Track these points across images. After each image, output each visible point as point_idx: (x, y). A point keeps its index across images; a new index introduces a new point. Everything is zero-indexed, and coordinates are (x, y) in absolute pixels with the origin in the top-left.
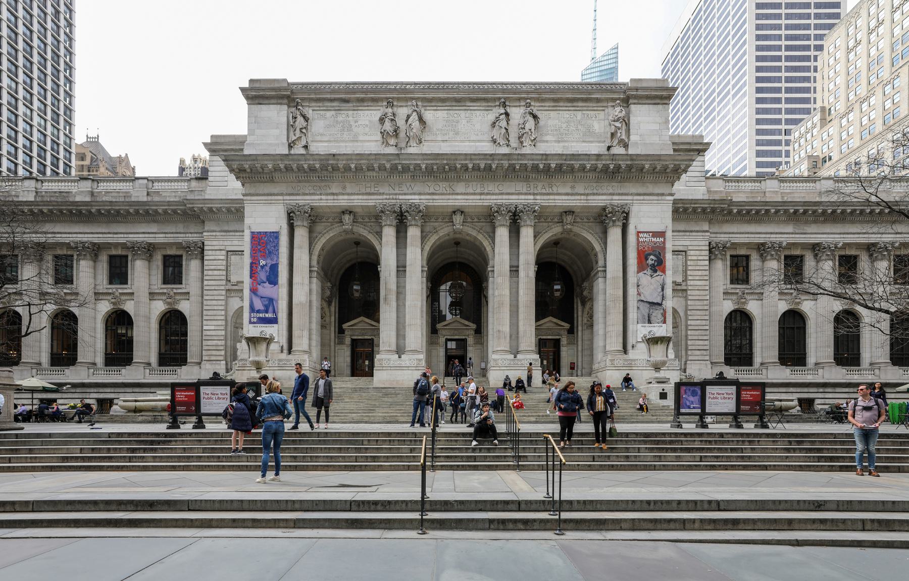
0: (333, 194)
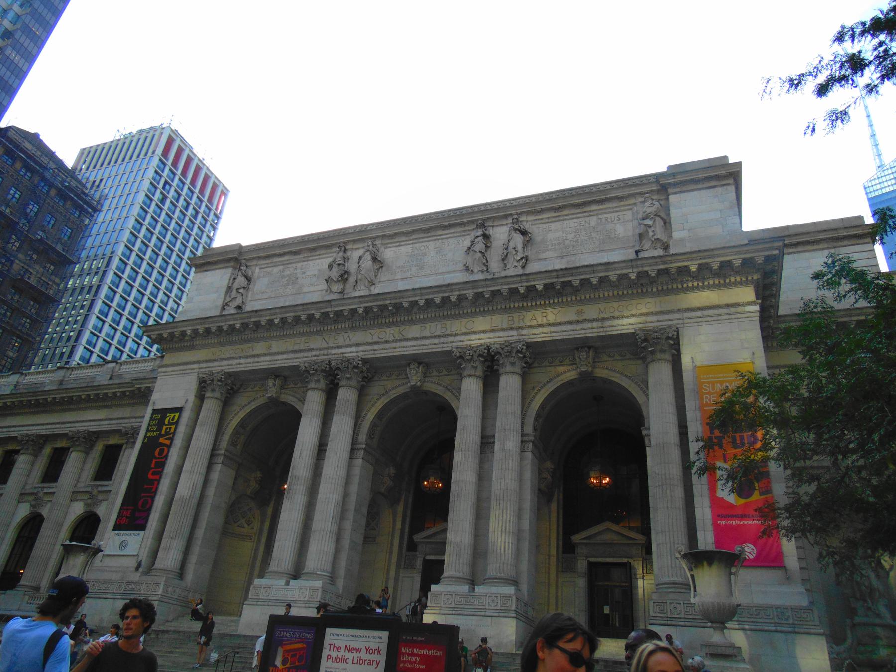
0: (254, 356)
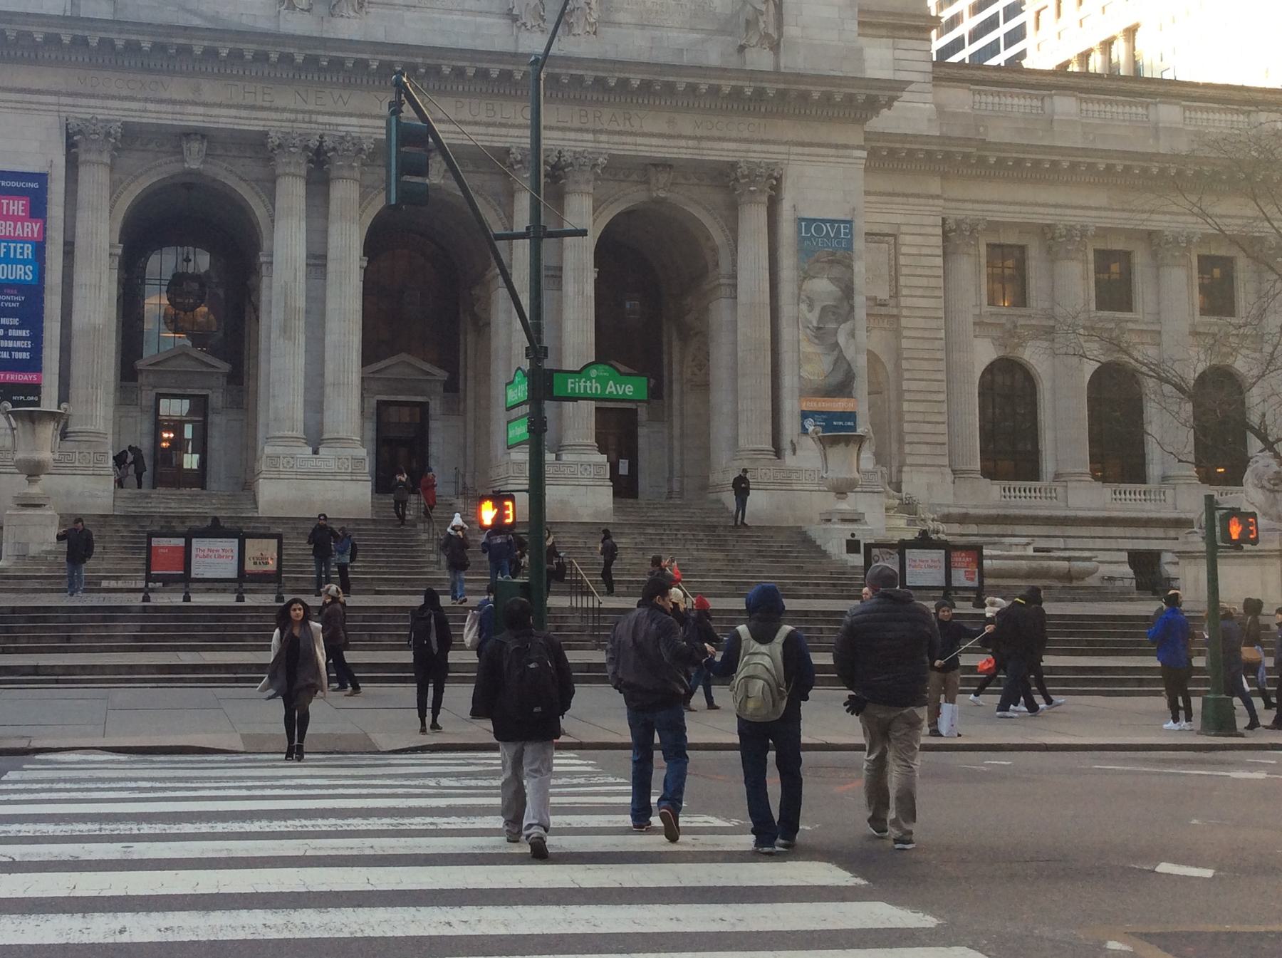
0: (173, 102)
